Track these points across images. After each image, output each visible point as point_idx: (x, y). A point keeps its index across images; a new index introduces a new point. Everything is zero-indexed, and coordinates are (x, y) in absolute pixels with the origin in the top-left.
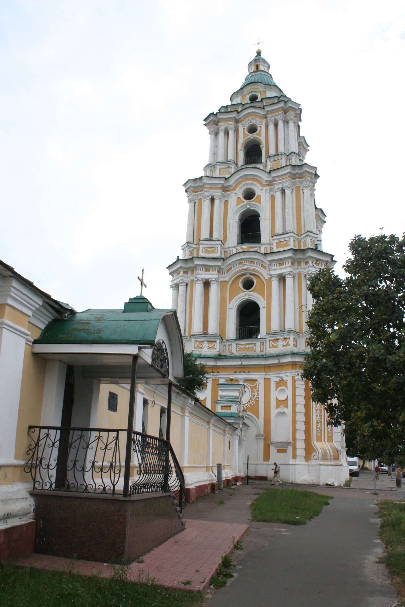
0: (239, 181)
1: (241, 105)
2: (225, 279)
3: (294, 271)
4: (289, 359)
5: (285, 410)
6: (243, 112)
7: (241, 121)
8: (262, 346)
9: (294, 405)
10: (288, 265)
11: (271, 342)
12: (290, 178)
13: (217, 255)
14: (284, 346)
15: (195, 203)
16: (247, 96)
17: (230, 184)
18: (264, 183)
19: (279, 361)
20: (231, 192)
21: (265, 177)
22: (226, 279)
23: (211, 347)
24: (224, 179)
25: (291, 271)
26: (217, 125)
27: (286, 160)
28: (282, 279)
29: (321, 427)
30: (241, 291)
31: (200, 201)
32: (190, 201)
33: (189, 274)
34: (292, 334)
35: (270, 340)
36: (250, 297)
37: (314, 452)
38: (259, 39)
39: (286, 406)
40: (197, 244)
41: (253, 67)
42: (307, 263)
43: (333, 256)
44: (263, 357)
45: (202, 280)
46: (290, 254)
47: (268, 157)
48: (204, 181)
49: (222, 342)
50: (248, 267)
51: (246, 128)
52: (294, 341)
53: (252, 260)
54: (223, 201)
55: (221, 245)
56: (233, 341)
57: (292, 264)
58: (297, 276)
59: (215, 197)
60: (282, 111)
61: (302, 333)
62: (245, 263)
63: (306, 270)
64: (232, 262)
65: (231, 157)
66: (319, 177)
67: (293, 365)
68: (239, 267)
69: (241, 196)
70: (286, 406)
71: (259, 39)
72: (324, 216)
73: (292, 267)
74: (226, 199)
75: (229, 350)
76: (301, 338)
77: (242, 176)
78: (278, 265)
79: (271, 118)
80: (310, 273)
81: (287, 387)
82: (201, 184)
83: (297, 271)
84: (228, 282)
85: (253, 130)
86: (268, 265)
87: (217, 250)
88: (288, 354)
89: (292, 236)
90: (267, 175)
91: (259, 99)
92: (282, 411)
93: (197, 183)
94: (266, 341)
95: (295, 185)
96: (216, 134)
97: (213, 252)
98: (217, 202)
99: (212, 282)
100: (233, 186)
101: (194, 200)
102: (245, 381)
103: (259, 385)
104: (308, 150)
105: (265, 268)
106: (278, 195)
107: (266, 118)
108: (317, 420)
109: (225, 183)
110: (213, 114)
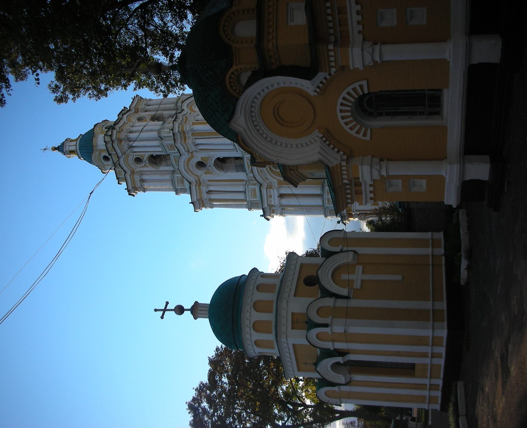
1: (116, 168)
13: (257, 188)
17: (194, 180)
21: (185, 156)
22: (276, 181)
48: (195, 200)
51: (138, 166)
54: (209, 183)
55: (248, 185)
65: (168, 177)
82: (197, 201)
84: (278, 180)
85: (138, 160)
97: (254, 190)
98: (211, 188)
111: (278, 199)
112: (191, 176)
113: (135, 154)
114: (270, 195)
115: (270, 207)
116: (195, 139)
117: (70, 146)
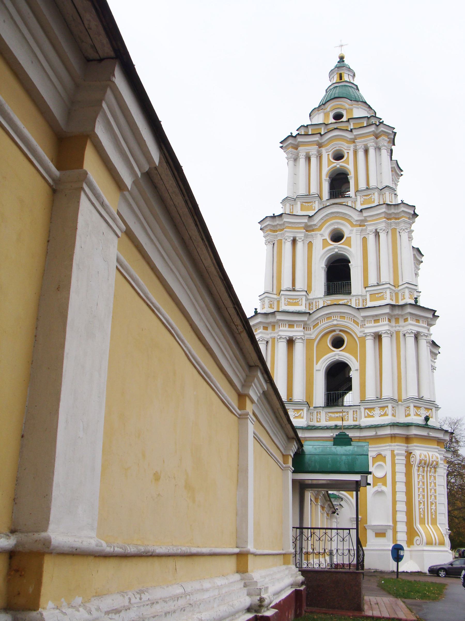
0: (325, 219)
1: (324, 125)
3: (391, 329)
4: (388, 431)
5: (383, 488)
6: (327, 134)
7: (326, 145)
8: (355, 414)
9: (394, 483)
10: (385, 323)
11: (366, 410)
12: (385, 219)
13: (302, 308)
14: (382, 415)
15: (274, 244)
16: (330, 114)
17: (315, 223)
18: (354, 223)
19: (376, 433)
20: (316, 232)
21: (355, 216)
22: (313, 336)
23: (297, 415)
24: (307, 217)
25: (389, 330)
26: (297, 149)
27: (379, 195)
28: (378, 337)
29: (424, 508)
31: (280, 241)
32: (267, 242)
33: (270, 330)
34: (391, 403)
35: (365, 409)
36: (340, 357)
37: (416, 536)
38: (341, 41)
39: (385, 484)
40: (278, 294)
41: (336, 75)
42: (406, 320)
43: (435, 311)
44: (358, 428)
46: (387, 310)
47: (357, 191)
48: (285, 220)
49: (309, 410)
50: (338, 322)
52: (392, 410)
53: (342, 315)
55: (305, 296)
56: (322, 408)
57: (389, 320)
58: (394, 335)
59: (297, 238)
60: (374, 136)
61: (401, 400)
62: (335, 318)
63: (405, 328)
64: (318, 317)
65: (314, 190)
66: (418, 215)
67: (392, 437)
68: (327, 323)
69: (327, 237)
70: (385, 484)
71: (341, 41)
72: (421, 256)
73: (388, 324)
74: (309, 240)
75: (317, 418)
76: (400, 407)
77: (328, 214)
78: (373, 321)
79: (360, 144)
80: (409, 332)
81: (385, 462)
82: (281, 223)
83: (394, 329)
84: (314, 340)
85: (339, 156)
86: (362, 321)
87: (302, 302)
88: (387, 426)
89: (389, 288)
90: (358, 213)
91: (344, 119)
92: (380, 490)
93: (276, 221)
94: (360, 409)
95: (391, 226)
96: (296, 160)
97: (296, 304)
98: (300, 245)
99: (297, 341)
100: (319, 225)
101: (272, 242)
104: (402, 175)
105: (357, 324)
106: (371, 239)
107: (354, 142)
109: (309, 221)
110: (291, 136)
111: (287, 336)
112: (321, 219)
115: (272, 324)
116: (387, 232)
117: (349, 75)
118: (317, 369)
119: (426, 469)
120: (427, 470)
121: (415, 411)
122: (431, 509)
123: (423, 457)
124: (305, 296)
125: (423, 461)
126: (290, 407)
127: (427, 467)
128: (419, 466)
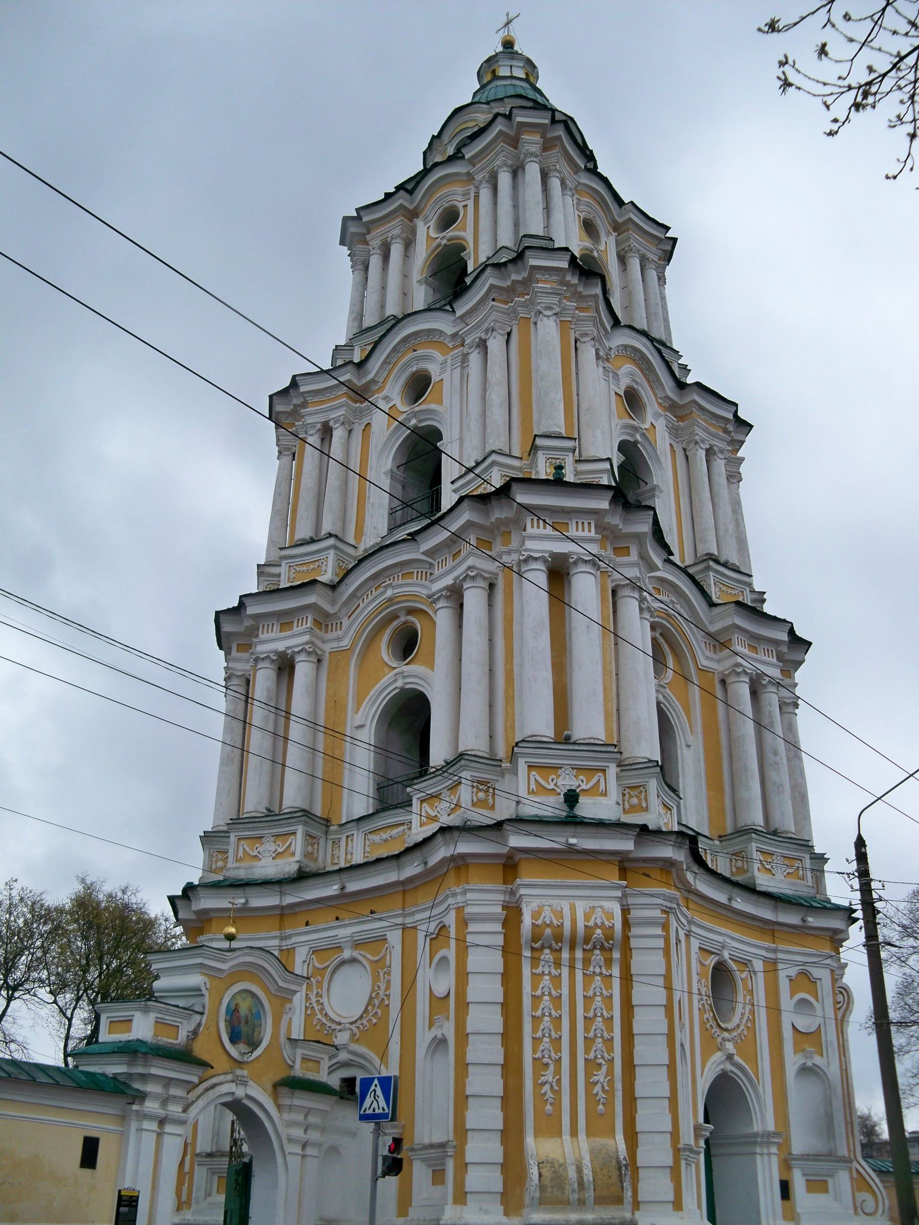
2: (343, 643)
22: (346, 643)
29: (559, 1081)
30: (386, 669)
45: (268, 657)
50: (396, 591)
55: (335, 547)
56: (355, 823)
75: (346, 853)
84: (351, 650)
100: (381, 380)
102: (357, 944)
103: (390, 952)
108: (539, 1055)
113: (470, 204)
114: (293, 622)
117: (511, 66)
118: (357, 724)
119: (565, 955)
120: (572, 960)
121: (533, 782)
122: (590, 1085)
123: (547, 916)
124: (335, 547)
125: (548, 931)
126: (266, 832)
127: (572, 948)
128: (536, 946)
